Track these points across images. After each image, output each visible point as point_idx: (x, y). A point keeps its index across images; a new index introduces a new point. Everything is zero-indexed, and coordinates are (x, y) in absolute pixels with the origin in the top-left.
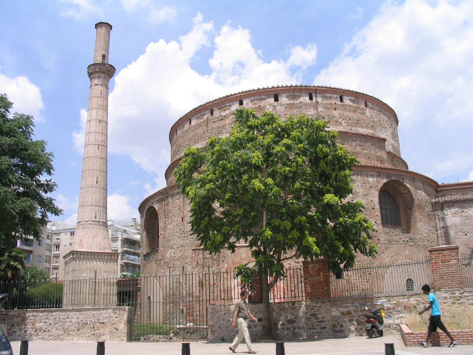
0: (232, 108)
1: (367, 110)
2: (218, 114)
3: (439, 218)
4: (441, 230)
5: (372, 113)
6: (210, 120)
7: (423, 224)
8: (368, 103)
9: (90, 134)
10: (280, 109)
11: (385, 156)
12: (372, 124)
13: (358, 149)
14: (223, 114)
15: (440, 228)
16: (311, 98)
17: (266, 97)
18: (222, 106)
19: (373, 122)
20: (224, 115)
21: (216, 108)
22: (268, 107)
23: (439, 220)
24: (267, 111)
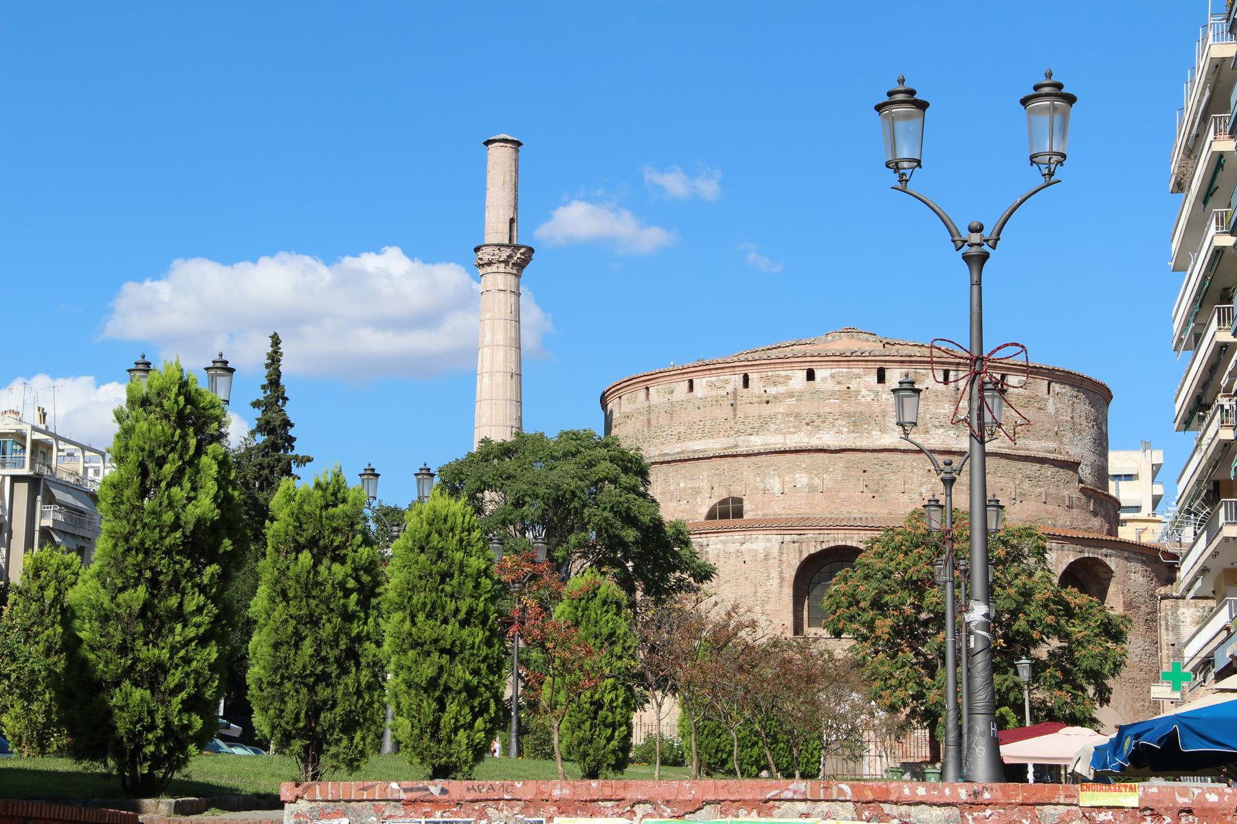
1: (1051, 400)
2: (759, 387)
3: (1167, 624)
4: (1168, 649)
5: (1058, 405)
6: (742, 397)
7: (1133, 639)
8: (1053, 384)
9: (494, 401)
10: (887, 399)
11: (1076, 494)
12: (1056, 429)
13: (1026, 485)
14: (772, 391)
15: (1167, 645)
16: (946, 381)
17: (861, 371)
18: (770, 374)
19: (1059, 424)
20: (774, 393)
22: (864, 392)
23: (1167, 629)
24: (863, 400)
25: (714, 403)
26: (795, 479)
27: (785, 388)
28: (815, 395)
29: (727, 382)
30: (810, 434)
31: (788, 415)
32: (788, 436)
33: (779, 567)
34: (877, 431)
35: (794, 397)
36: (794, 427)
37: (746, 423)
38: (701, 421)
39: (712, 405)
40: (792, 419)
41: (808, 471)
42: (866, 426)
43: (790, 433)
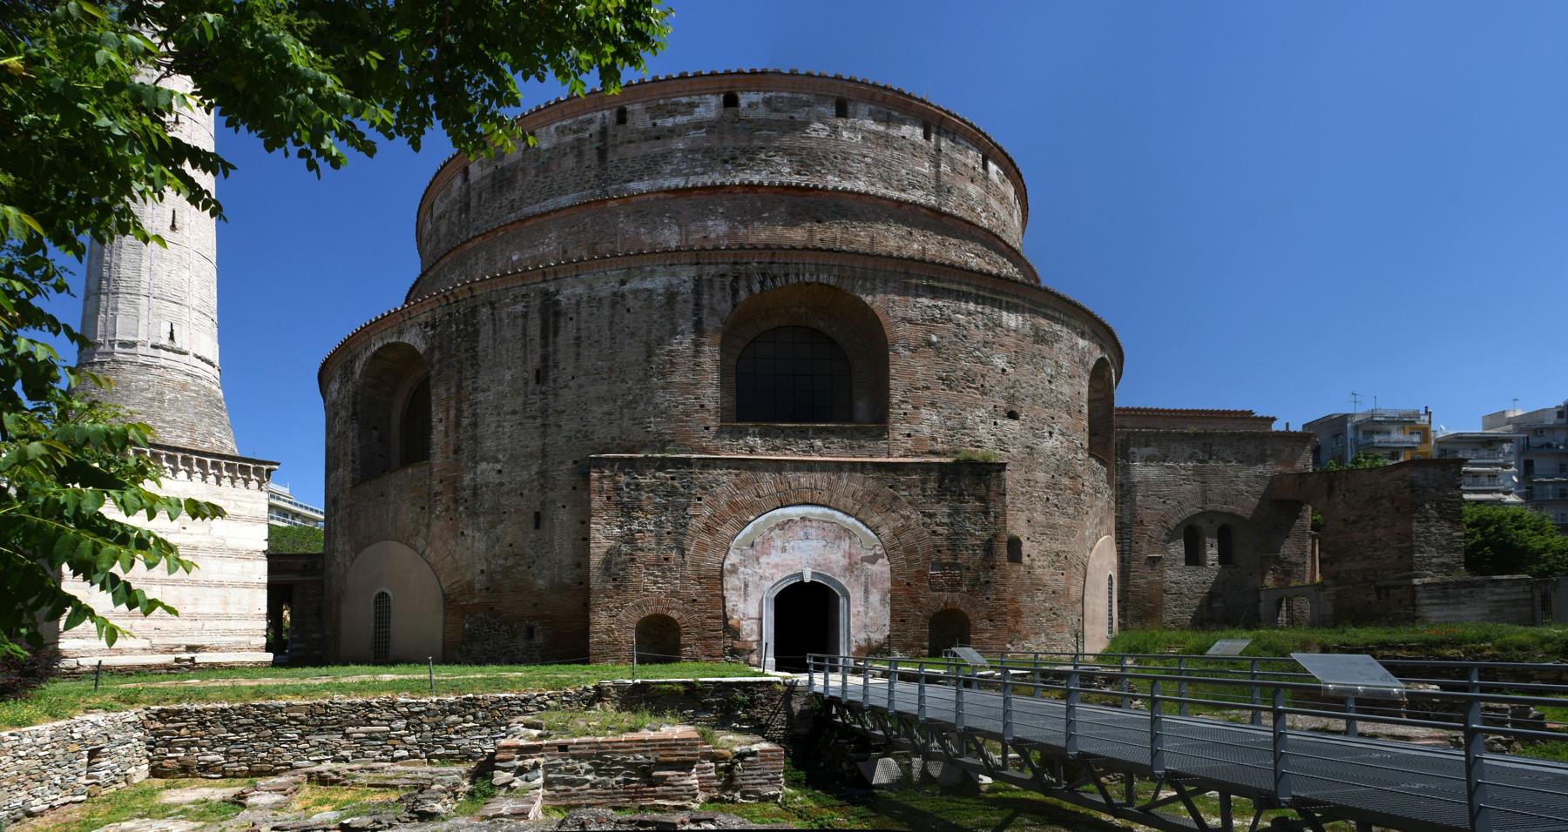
0: (696, 109)
18: (661, 102)
21: (638, 107)
25: (568, 150)
26: (705, 228)
27: (689, 117)
28: (737, 125)
29: (590, 121)
30: (726, 173)
31: (691, 151)
32: (691, 178)
33: (695, 315)
34: (834, 175)
35: (702, 128)
36: (702, 166)
37: (622, 168)
38: (546, 178)
39: (565, 154)
40: (699, 156)
41: (727, 216)
42: (819, 168)
43: (696, 174)
